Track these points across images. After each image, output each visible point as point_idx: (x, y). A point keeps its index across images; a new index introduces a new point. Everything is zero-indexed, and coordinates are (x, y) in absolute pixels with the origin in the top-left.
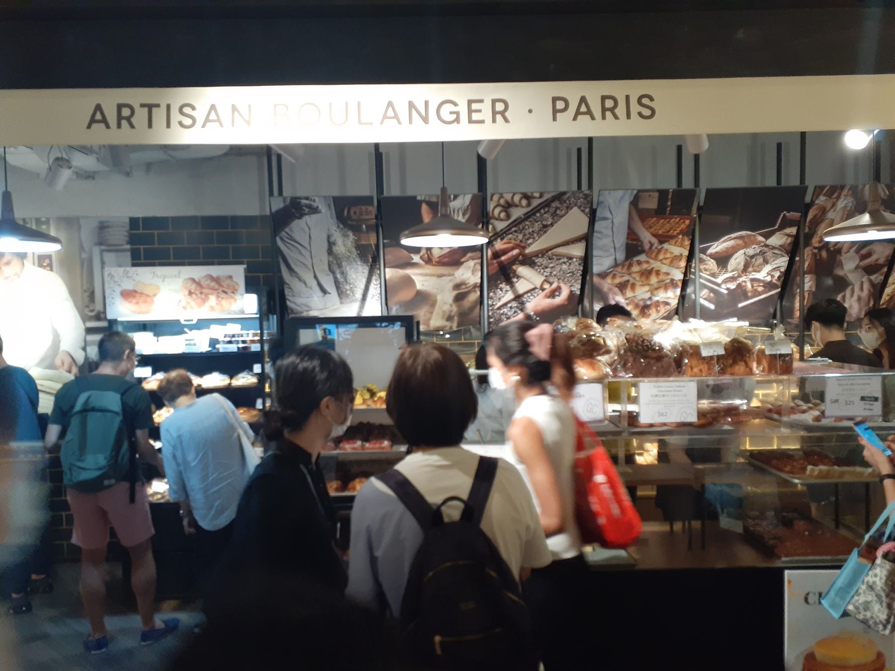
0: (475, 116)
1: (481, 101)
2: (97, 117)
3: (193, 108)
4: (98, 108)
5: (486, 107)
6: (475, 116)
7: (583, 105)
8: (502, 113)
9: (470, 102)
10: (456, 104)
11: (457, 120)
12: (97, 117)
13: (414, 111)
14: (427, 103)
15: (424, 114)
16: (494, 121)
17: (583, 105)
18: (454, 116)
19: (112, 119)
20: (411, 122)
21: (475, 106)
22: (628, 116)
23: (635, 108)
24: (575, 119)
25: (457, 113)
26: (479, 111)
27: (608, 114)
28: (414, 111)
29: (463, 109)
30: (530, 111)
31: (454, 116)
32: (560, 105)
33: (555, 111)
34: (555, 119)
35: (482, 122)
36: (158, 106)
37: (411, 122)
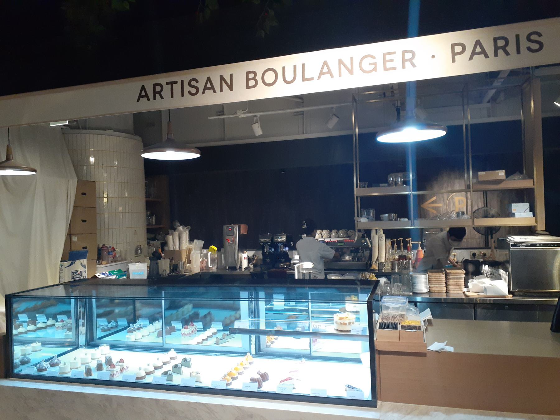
0: (389, 65)
1: (394, 53)
2: (143, 94)
3: (197, 81)
4: (143, 88)
5: (398, 58)
6: (389, 65)
7: (478, 47)
9: (385, 55)
10: (374, 57)
11: (375, 69)
12: (143, 94)
13: (342, 66)
15: (350, 67)
16: (404, 67)
17: (478, 47)
18: (373, 66)
19: (151, 95)
20: (340, 75)
21: (388, 57)
22: (518, 52)
23: (524, 44)
24: (471, 58)
25: (375, 64)
26: (392, 60)
27: (500, 52)
28: (342, 66)
30: (433, 57)
31: (373, 66)
32: (458, 49)
33: (454, 54)
35: (394, 68)
37: (340, 75)
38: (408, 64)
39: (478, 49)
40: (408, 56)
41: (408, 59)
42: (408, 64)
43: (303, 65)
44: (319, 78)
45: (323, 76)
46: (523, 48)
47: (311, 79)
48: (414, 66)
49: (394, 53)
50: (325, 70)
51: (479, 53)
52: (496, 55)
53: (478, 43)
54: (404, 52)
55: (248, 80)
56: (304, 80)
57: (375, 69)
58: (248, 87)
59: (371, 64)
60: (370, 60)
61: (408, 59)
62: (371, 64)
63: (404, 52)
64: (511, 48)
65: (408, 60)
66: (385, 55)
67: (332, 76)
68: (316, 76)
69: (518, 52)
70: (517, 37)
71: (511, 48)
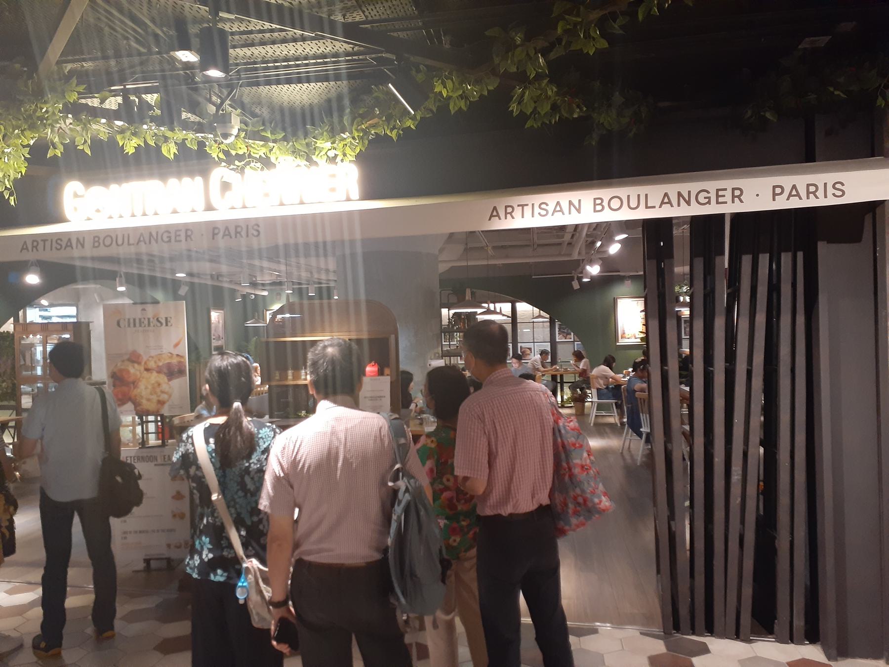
0: (721, 200)
1: (725, 189)
6: (721, 200)
8: (739, 197)
9: (718, 190)
10: (708, 192)
11: (709, 203)
14: (689, 192)
16: (733, 202)
21: (720, 193)
24: (788, 199)
25: (709, 198)
26: (724, 196)
30: (757, 195)
33: (775, 195)
34: (774, 200)
35: (726, 203)
36: (527, 205)
38: (736, 199)
40: (737, 193)
42: (736, 199)
43: (646, 195)
44: (660, 207)
46: (829, 194)
47: (654, 207)
48: (741, 201)
49: (725, 189)
51: (794, 196)
54: (734, 189)
55: (595, 205)
56: (647, 207)
57: (709, 203)
58: (595, 211)
60: (706, 195)
63: (734, 189)
66: (718, 190)
67: (672, 206)
68: (658, 206)
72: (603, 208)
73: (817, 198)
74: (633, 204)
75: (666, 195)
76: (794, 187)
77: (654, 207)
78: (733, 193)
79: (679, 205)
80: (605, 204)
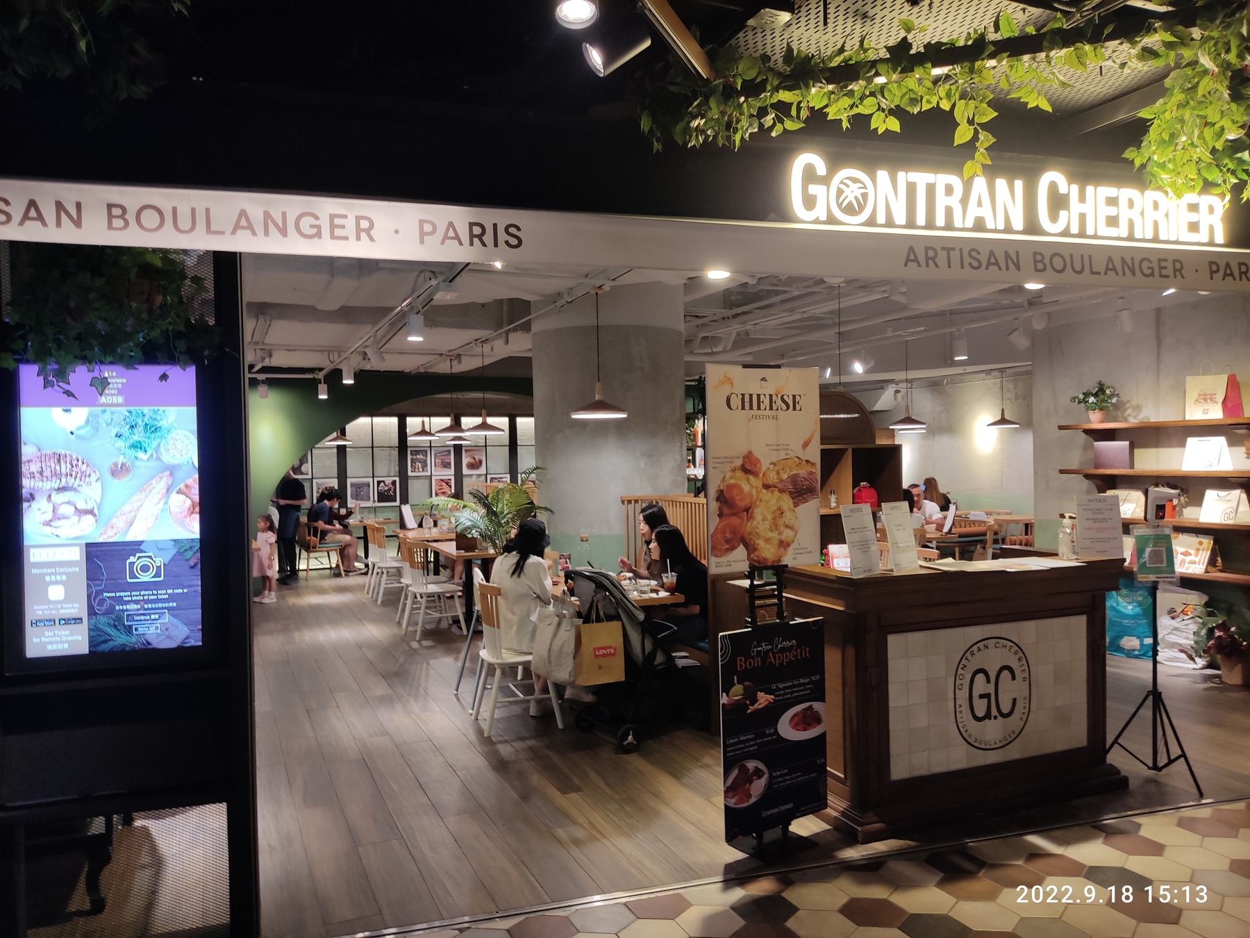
0: (338, 232)
1: (345, 217)
5: (350, 223)
8: (368, 231)
9: (332, 217)
10: (317, 218)
11: (319, 235)
14: (284, 214)
16: (358, 238)
18: (314, 231)
21: (337, 221)
24: (443, 243)
25: (319, 227)
26: (343, 227)
27: (476, 240)
29: (325, 223)
30: (397, 232)
31: (314, 231)
32: (428, 228)
33: (423, 234)
35: (347, 238)
39: (451, 234)
41: (365, 230)
42: (363, 235)
43: (208, 210)
45: (239, 232)
48: (372, 239)
49: (345, 217)
50: (243, 223)
52: (471, 244)
53: (451, 225)
57: (319, 235)
59: (311, 226)
61: (365, 230)
62: (311, 226)
64: (489, 238)
65: (364, 230)
66: (332, 217)
67: (254, 234)
69: (496, 245)
70: (495, 225)
71: (489, 238)
72: (127, 223)
73: (484, 245)
74: (185, 223)
75: (243, 213)
76: (451, 225)
77: (223, 233)
78: (358, 225)
79: (267, 233)
80: (131, 216)
